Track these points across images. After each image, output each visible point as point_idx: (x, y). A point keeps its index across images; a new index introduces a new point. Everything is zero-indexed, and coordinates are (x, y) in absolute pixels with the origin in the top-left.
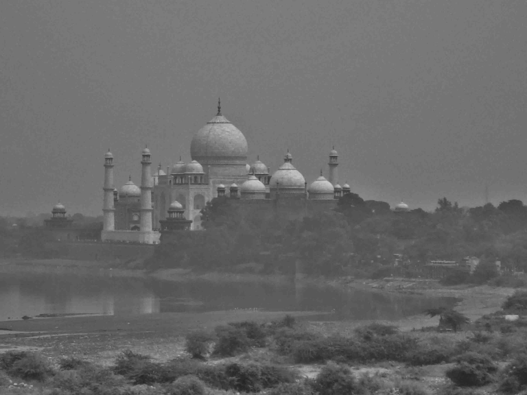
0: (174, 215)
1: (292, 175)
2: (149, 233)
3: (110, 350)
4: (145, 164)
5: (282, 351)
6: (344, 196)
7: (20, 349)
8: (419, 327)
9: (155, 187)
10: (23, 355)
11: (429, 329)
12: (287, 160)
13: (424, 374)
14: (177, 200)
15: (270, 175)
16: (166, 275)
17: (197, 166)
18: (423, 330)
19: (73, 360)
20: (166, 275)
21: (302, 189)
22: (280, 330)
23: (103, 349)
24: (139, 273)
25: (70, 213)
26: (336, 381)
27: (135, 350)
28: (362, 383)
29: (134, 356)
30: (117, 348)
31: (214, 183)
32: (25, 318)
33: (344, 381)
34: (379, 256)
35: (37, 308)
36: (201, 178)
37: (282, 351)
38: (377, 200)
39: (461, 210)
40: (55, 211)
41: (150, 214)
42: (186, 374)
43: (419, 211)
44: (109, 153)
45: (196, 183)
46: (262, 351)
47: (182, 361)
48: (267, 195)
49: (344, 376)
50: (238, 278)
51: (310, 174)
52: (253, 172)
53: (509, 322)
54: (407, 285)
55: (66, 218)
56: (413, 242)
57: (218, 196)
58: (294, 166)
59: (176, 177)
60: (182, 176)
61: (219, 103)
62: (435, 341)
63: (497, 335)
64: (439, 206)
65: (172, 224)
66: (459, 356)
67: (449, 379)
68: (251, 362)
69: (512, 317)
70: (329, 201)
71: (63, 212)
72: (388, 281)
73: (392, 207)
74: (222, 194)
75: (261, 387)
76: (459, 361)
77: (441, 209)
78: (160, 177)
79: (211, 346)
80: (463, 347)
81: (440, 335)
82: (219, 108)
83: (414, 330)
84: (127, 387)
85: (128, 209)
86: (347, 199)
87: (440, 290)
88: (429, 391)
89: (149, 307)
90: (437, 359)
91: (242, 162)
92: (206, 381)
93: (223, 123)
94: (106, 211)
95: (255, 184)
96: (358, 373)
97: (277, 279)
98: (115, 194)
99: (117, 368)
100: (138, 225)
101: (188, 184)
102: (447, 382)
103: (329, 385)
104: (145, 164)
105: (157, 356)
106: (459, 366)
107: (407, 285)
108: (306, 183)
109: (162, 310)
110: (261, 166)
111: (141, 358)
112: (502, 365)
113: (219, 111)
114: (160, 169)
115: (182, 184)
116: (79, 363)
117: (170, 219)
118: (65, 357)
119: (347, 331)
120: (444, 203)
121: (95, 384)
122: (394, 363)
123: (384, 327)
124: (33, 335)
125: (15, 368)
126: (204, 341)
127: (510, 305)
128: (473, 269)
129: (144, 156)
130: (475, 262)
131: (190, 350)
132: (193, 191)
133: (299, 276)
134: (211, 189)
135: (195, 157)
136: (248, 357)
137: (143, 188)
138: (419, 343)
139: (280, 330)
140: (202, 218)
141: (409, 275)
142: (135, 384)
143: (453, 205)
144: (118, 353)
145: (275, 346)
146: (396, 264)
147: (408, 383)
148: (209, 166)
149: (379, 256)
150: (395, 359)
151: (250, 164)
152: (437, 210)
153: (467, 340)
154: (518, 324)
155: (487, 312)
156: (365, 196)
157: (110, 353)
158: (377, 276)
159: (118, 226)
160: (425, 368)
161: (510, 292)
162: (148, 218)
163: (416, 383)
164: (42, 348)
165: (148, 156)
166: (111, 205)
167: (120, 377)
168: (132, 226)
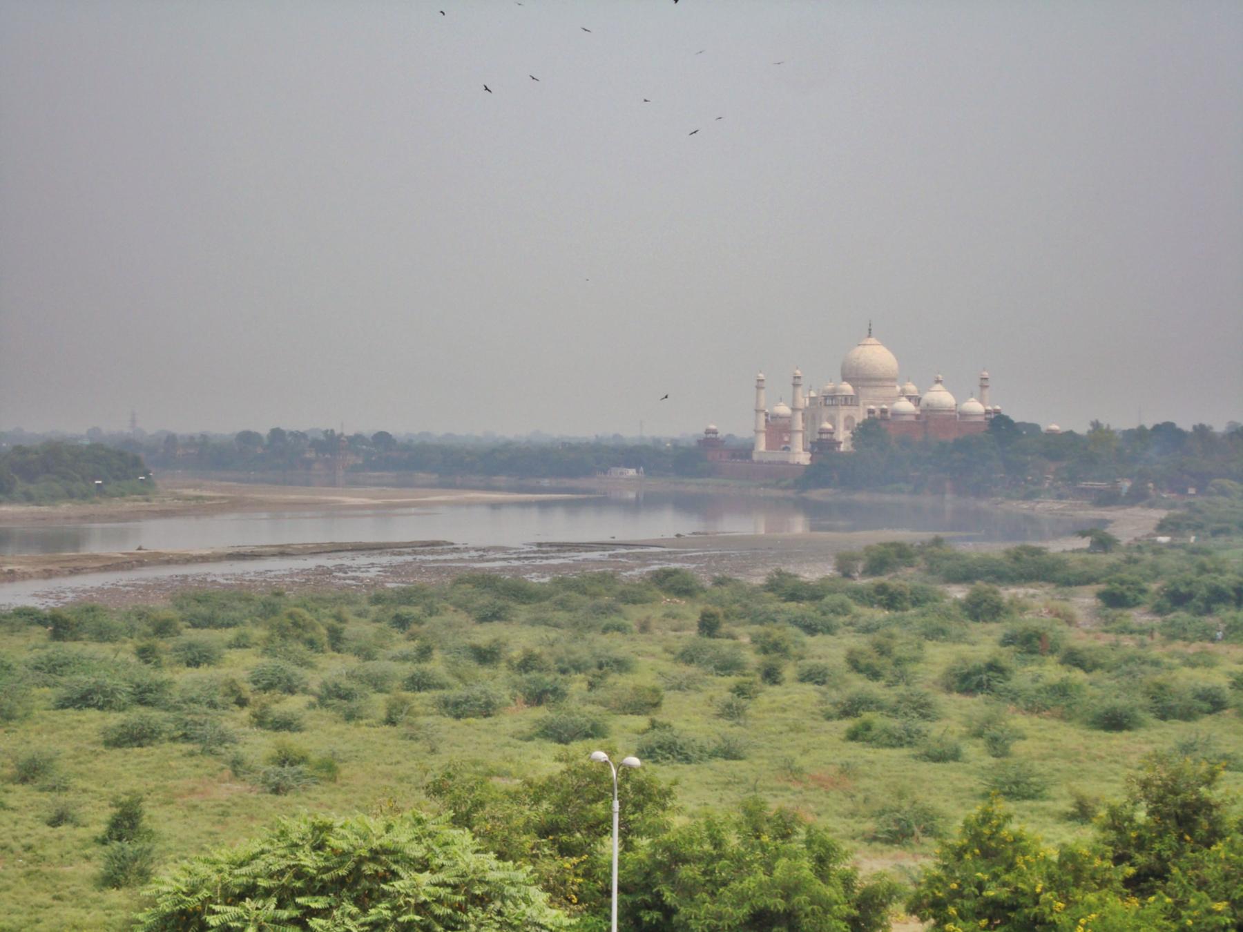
1: (942, 397)
4: (795, 385)
8: (1069, 547)
9: (806, 408)
11: (1079, 551)
12: (938, 381)
17: (847, 388)
18: (1073, 551)
24: (790, 493)
25: (722, 434)
27: (784, 569)
28: (1011, 603)
37: (931, 571)
38: (1028, 421)
39: (1113, 432)
40: (708, 432)
41: (800, 436)
42: (835, 592)
45: (846, 404)
46: (910, 571)
47: (831, 579)
48: (917, 417)
52: (902, 393)
53: (1160, 544)
55: (716, 439)
59: (826, 398)
60: (833, 397)
62: (1086, 562)
63: (1149, 557)
65: (822, 446)
69: (1164, 539)
73: (1044, 429)
76: (1109, 582)
78: (811, 398)
79: (860, 566)
80: (1114, 568)
81: (1090, 557)
83: (1064, 551)
84: (777, 604)
85: (778, 429)
90: (1090, 580)
94: (757, 432)
95: (905, 406)
96: (1007, 593)
98: (767, 415)
103: (978, 605)
104: (795, 385)
105: (807, 575)
109: (812, 529)
110: (912, 388)
111: (790, 576)
112: (1153, 587)
116: (730, 580)
117: (820, 440)
118: (717, 574)
119: (995, 549)
120: (1096, 425)
121: (745, 601)
125: (667, 584)
126: (854, 559)
127: (1162, 528)
128: (1125, 491)
130: (1126, 485)
131: (840, 567)
132: (843, 412)
133: (948, 496)
135: (845, 378)
137: (794, 409)
141: (1060, 497)
143: (1105, 427)
144: (769, 570)
145: (923, 565)
150: (1044, 579)
153: (1117, 562)
154: (1171, 546)
155: (1139, 534)
156: (1016, 418)
158: (1029, 496)
159: (769, 446)
160: (1074, 589)
161: (1161, 514)
162: (798, 441)
163: (1066, 604)
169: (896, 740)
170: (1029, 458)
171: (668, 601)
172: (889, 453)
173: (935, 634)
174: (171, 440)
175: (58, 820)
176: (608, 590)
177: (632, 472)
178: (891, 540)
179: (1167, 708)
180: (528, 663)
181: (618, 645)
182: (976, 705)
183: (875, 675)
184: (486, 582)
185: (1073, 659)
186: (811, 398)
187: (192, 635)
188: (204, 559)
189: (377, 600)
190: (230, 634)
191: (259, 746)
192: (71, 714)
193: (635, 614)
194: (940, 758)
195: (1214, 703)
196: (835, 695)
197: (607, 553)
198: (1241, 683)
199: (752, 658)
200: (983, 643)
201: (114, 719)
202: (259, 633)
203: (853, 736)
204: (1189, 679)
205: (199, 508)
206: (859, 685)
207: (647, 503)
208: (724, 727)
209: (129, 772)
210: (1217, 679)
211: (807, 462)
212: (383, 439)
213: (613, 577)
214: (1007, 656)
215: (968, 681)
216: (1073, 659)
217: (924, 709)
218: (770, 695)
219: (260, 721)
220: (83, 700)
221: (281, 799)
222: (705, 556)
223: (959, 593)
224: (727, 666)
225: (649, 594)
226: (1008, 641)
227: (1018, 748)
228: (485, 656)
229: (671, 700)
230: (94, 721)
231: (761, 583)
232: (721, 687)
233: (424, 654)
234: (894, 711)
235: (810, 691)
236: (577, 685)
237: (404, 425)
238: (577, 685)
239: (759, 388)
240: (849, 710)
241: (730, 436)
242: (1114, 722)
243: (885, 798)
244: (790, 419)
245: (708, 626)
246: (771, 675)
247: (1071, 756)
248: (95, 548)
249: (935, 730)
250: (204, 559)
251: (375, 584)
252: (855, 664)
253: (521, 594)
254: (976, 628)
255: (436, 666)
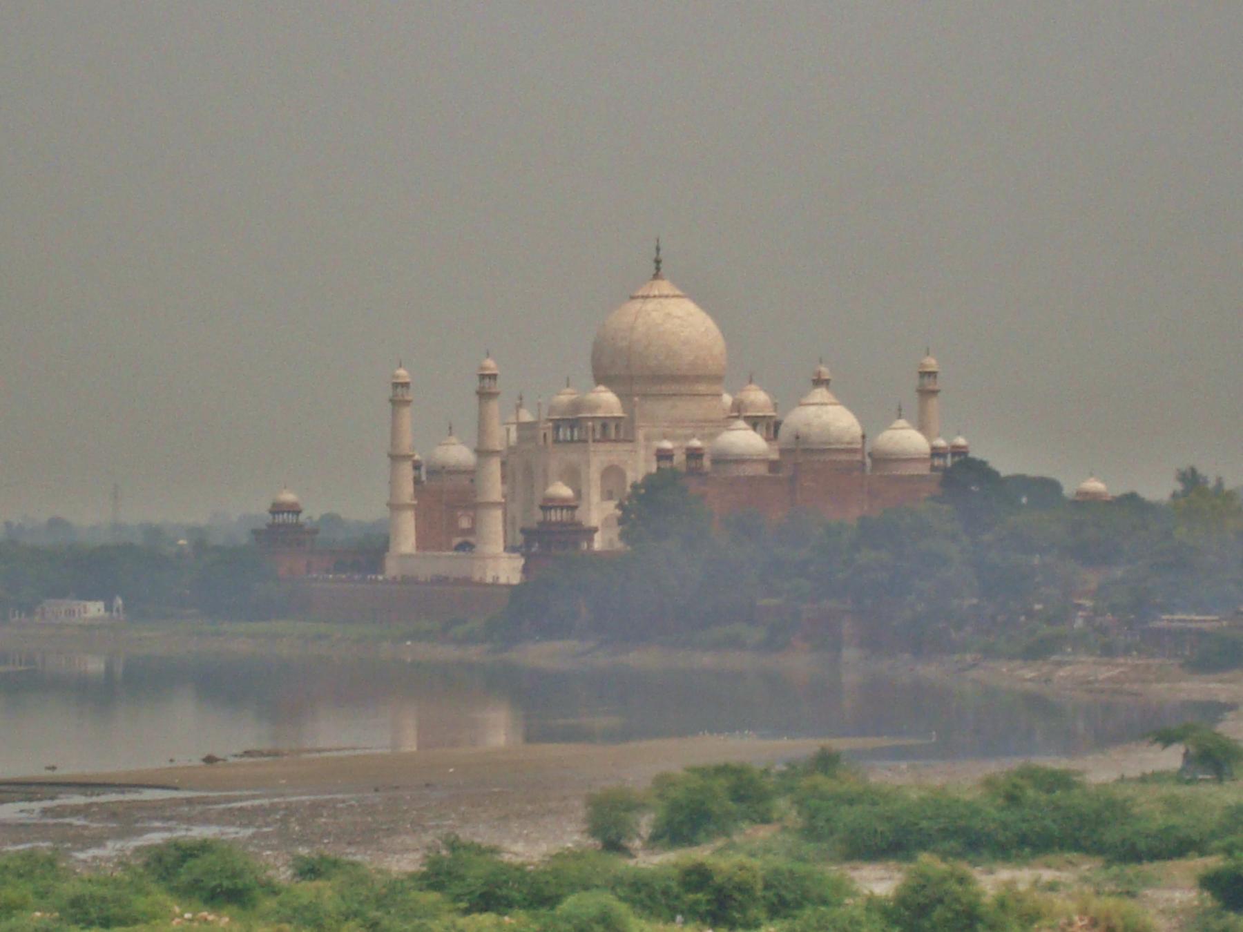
0: (555, 516)
2: (495, 557)
3: (407, 833)
4: (484, 395)
5: (811, 832)
6: (954, 465)
7: (200, 832)
8: (1133, 771)
9: (511, 450)
10: (204, 847)
11: (1158, 777)
12: (819, 382)
13: (1147, 882)
14: (561, 478)
15: (778, 418)
16: (541, 655)
17: (607, 400)
18: (1143, 779)
19: (322, 858)
20: (541, 655)
21: (854, 451)
22: (805, 782)
23: (391, 832)
24: (473, 653)
25: (312, 513)
26: (941, 901)
27: (465, 835)
28: (1002, 905)
29: (465, 847)
30: (425, 830)
31: (648, 438)
32: (210, 760)
33: (957, 900)
34: (1038, 607)
35: (236, 736)
36: (617, 427)
37: (811, 832)
38: (1032, 471)
39: (1230, 495)
40: (277, 509)
41: (498, 514)
42: (586, 888)
43: (1131, 500)
44: (402, 372)
45: (605, 439)
46: (764, 833)
47: (577, 856)
48: (773, 466)
49: (958, 888)
50: (707, 660)
51: (874, 414)
52: (739, 411)
54: (1105, 673)
55: (299, 527)
56: (1119, 573)
57: (659, 468)
58: (836, 395)
60: (574, 423)
61: (658, 249)
62: (1173, 805)
64: (1178, 487)
65: (551, 537)
66: (1230, 839)
67: (1206, 894)
68: (740, 858)
70: (922, 477)
71: (295, 510)
72: (1060, 664)
73: (1069, 490)
74: (666, 465)
75: (762, 916)
76: (1229, 851)
77: (1185, 493)
78: (521, 426)
79: (645, 824)
81: (1183, 791)
82: (658, 262)
83: (1122, 779)
84: (446, 920)
85: (446, 501)
86: (960, 473)
87: (1183, 685)
88: (1161, 923)
89: (498, 731)
90: (1180, 847)
91: (715, 388)
92: (632, 902)
93: (667, 297)
94: (395, 507)
95: (744, 439)
96: (991, 881)
97: (799, 663)
98: (417, 466)
99: (424, 876)
100: (471, 539)
101: (585, 441)
102: (1202, 902)
103: (923, 910)
104: (484, 395)
106: (1231, 863)
107: (1105, 673)
108: (863, 437)
109: (528, 739)
110: (758, 397)
111: (480, 851)
113: (658, 269)
114: (519, 406)
115: (572, 441)
116: (335, 864)
117: (544, 523)
118: (303, 851)
119: (965, 781)
120: (1191, 479)
121: (374, 914)
122: (1073, 856)
123: (1054, 773)
124: (229, 800)
125: (184, 878)
129: (483, 377)
132: (599, 458)
133: (850, 654)
134: (642, 453)
135: (602, 377)
136: (731, 846)
137: (483, 453)
138: (1136, 810)
139: (805, 782)
140: (621, 521)
141: (1108, 651)
142: (467, 912)
143: (1212, 484)
144: (428, 838)
145: (794, 818)
146: (1079, 623)
147: (1111, 902)
148: (636, 399)
149: (1038, 607)
150: (1077, 846)
151: (732, 392)
152: (1174, 495)
156: (1005, 464)
157: (409, 840)
158: (1037, 651)
159: (423, 542)
160: (1149, 868)
162: (494, 524)
163: (1128, 904)
164: (250, 831)
165: (493, 377)
166: (407, 491)
167: (433, 896)
168: (457, 540)
170: (1036, 560)
176: (42, 895)
177: (95, 609)
178: (720, 760)
186: (521, 426)
197: (36, 806)
211: (516, 579)
213: (51, 862)
222: (274, 808)
225: (141, 904)
231: (412, 868)
239: (397, 403)
241: (331, 520)
244: (471, 474)
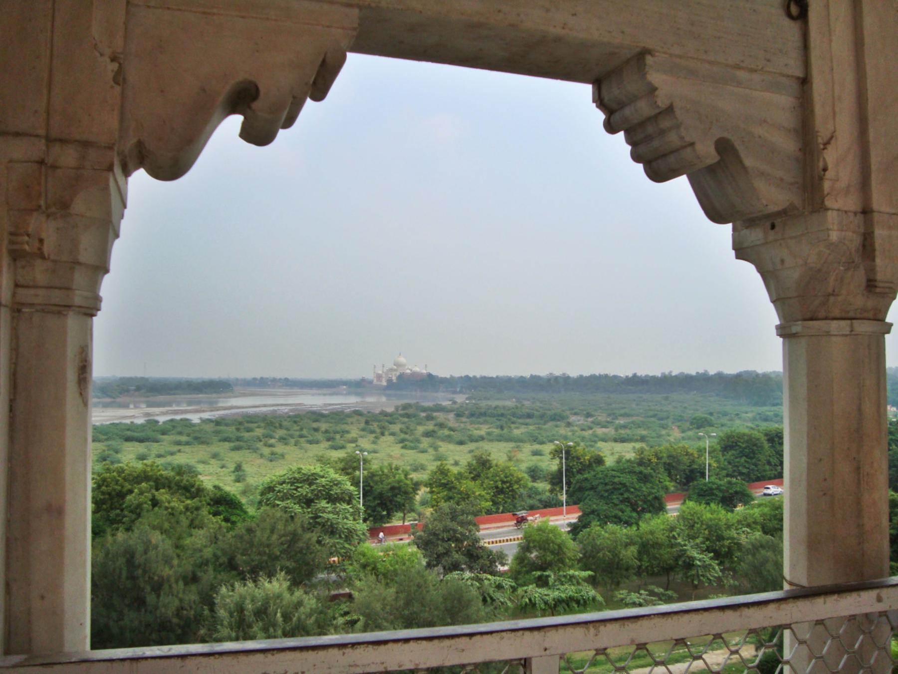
1: (417, 369)
65: (389, 381)
85: (379, 377)
90: (451, 411)
95: (408, 371)
96: (435, 414)
97: (414, 393)
107: (443, 394)
127: (467, 399)
161: (467, 396)
169: (412, 448)
171: (356, 417)
172: (406, 382)
173: (419, 424)
174: (237, 380)
175: (223, 467)
179: (473, 439)
180: (326, 432)
181: (347, 427)
182: (430, 440)
183: (406, 433)
184: (314, 413)
185: (451, 429)
187: (247, 425)
188: (246, 407)
189: (289, 417)
190: (256, 425)
191: (266, 451)
192: (222, 443)
193: (349, 420)
194: (422, 452)
195: (482, 438)
196: (399, 438)
198: (489, 434)
199: (378, 431)
200: (430, 426)
201: (232, 444)
202: (262, 425)
203: (403, 448)
204: (477, 433)
205: (244, 395)
206: (403, 436)
207: (349, 394)
208: (374, 446)
209: (237, 456)
210: (482, 433)
212: (286, 379)
214: (436, 428)
215: (427, 434)
216: (451, 429)
217: (418, 441)
218: (383, 439)
219: (266, 445)
220: (226, 440)
221: (273, 463)
223: (423, 414)
224: (372, 432)
226: (435, 425)
227: (440, 449)
228: (316, 430)
229: (360, 440)
230: (227, 445)
232: (372, 437)
233: (301, 429)
234: (411, 442)
235: (392, 438)
236: (338, 436)
237: (291, 376)
238: (338, 436)
240: (402, 441)
242: (461, 443)
243: (411, 462)
245: (367, 422)
246: (383, 434)
247: (452, 451)
248: (221, 405)
249: (422, 446)
250: (246, 407)
251: (286, 413)
252: (401, 431)
253: (323, 416)
254: (428, 423)
255: (305, 432)
